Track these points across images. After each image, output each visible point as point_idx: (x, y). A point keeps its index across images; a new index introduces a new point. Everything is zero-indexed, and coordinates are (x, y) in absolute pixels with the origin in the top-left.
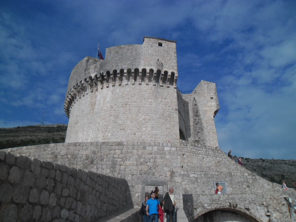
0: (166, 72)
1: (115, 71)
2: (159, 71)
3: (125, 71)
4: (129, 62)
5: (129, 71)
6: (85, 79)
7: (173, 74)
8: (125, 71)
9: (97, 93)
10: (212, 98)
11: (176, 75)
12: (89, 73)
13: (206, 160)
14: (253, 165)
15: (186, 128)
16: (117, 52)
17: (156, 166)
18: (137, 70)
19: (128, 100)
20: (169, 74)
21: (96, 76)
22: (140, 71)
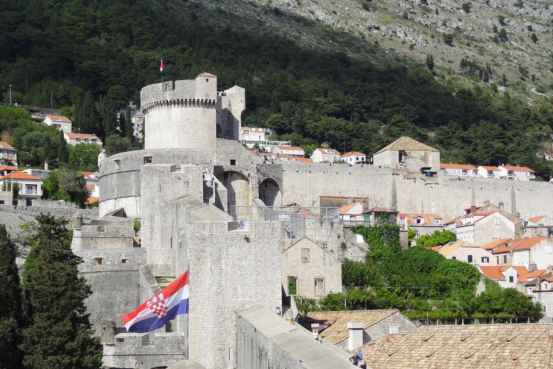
0: (210, 100)
1: (182, 100)
2: (206, 100)
3: (188, 100)
4: (189, 94)
5: (190, 100)
6: (164, 101)
7: (214, 100)
8: (188, 100)
9: (171, 110)
10: (242, 101)
11: (216, 101)
12: (166, 97)
13: (230, 147)
14: (533, 19)
15: (223, 122)
16: (183, 86)
17: (206, 158)
18: (194, 100)
19: (189, 117)
20: (212, 101)
21: (171, 101)
22: (196, 100)
